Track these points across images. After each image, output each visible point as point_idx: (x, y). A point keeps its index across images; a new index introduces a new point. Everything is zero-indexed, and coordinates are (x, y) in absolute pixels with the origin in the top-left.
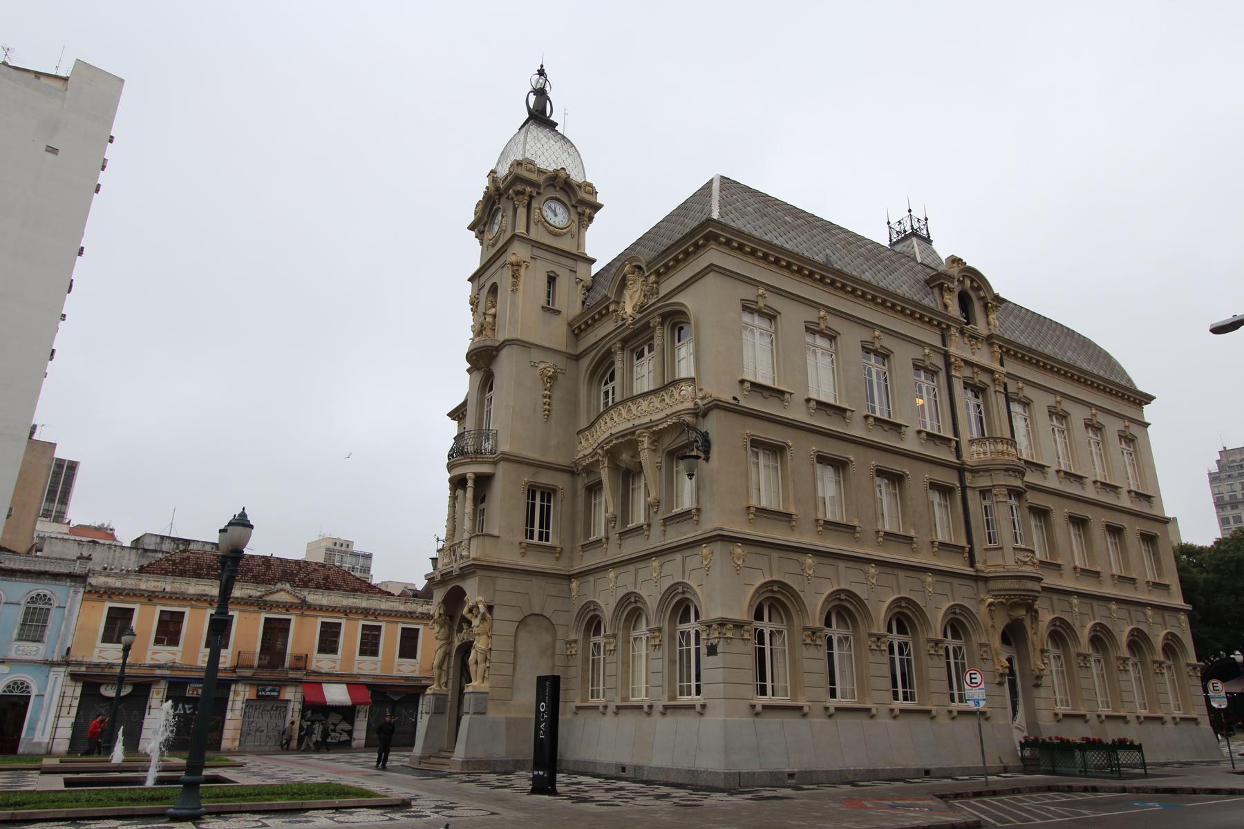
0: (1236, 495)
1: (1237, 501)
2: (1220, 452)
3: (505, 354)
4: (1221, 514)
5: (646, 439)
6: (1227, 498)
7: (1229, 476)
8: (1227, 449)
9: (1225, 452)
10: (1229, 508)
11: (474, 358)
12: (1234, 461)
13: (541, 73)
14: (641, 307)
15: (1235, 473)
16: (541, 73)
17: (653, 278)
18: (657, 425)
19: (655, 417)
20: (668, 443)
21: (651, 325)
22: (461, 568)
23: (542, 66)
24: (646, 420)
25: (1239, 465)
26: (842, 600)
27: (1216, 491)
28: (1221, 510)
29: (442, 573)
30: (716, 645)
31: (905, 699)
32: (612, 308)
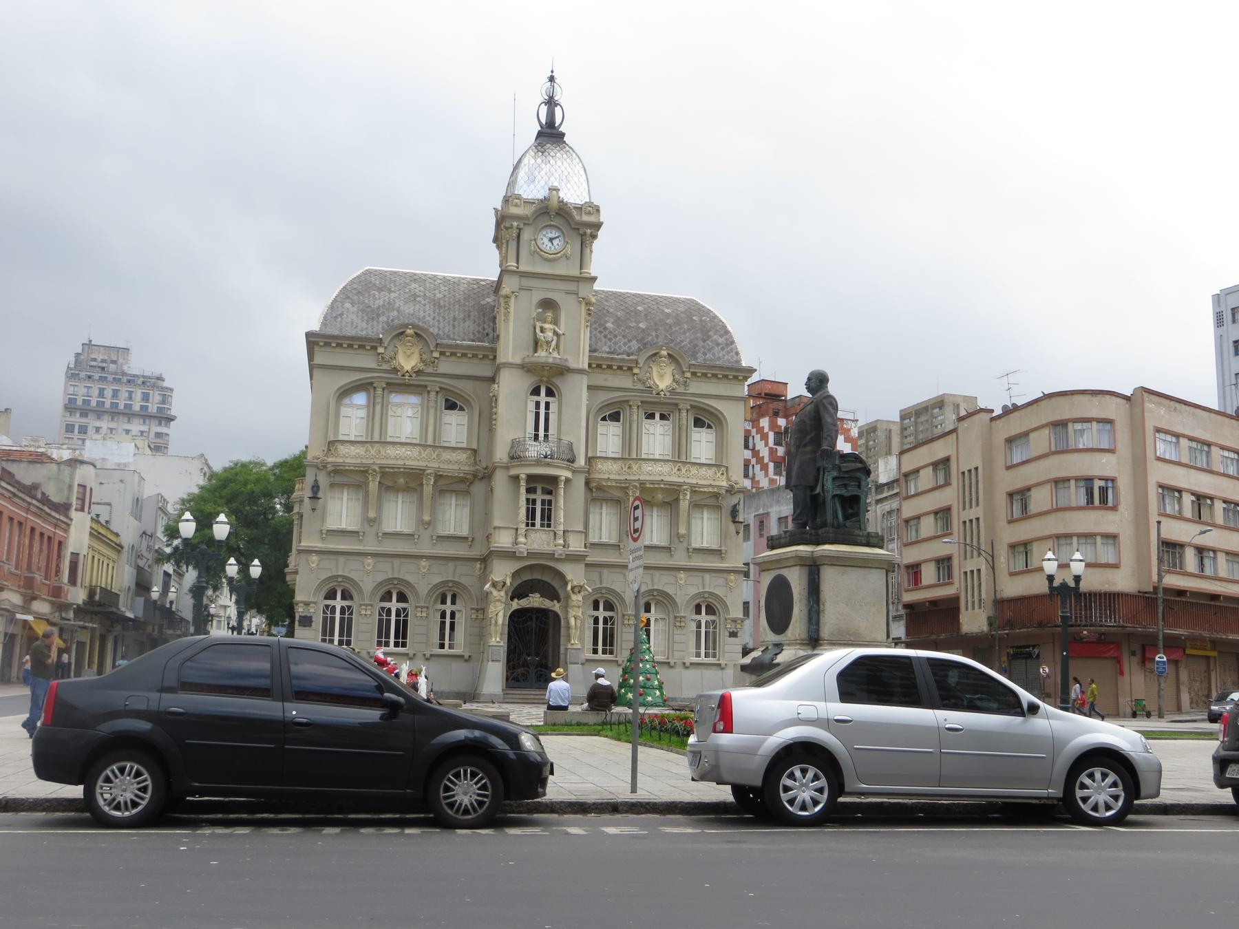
0: (90, 400)
1: (90, 408)
2: (83, 344)
3: (577, 377)
4: (67, 419)
5: (688, 493)
6: (79, 402)
7: (89, 377)
8: (93, 343)
9: (89, 345)
10: (78, 415)
11: (548, 368)
12: (95, 360)
13: (552, 79)
14: (673, 389)
15: (96, 376)
16: (552, 79)
17: (688, 375)
18: (699, 488)
19: (700, 482)
20: (696, 498)
21: (680, 407)
22: (566, 555)
23: (552, 72)
24: (694, 481)
25: (99, 367)
26: (655, 596)
27: (71, 390)
28: (69, 414)
29: (529, 551)
30: (737, 633)
31: (449, 648)
32: (636, 371)
